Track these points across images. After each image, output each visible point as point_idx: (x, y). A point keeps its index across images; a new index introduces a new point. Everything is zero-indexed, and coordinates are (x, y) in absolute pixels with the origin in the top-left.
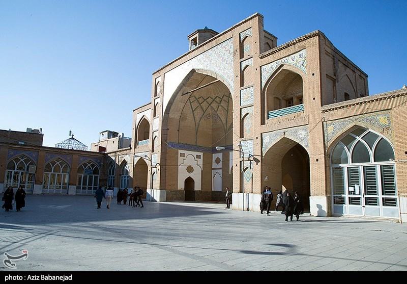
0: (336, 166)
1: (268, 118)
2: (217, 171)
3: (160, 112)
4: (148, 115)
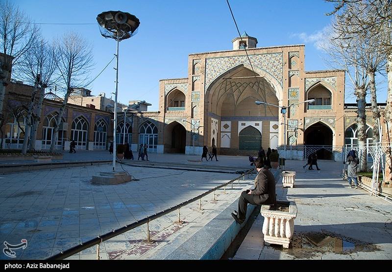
0: (349, 138)
1: (308, 109)
2: (226, 133)
3: (200, 89)
4: (185, 88)
